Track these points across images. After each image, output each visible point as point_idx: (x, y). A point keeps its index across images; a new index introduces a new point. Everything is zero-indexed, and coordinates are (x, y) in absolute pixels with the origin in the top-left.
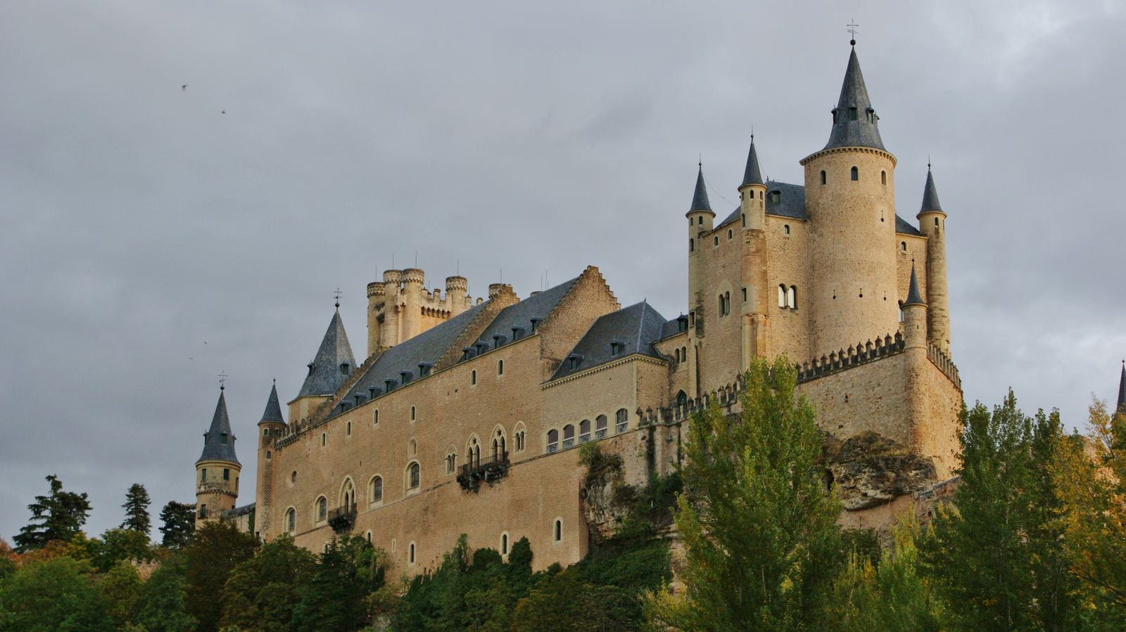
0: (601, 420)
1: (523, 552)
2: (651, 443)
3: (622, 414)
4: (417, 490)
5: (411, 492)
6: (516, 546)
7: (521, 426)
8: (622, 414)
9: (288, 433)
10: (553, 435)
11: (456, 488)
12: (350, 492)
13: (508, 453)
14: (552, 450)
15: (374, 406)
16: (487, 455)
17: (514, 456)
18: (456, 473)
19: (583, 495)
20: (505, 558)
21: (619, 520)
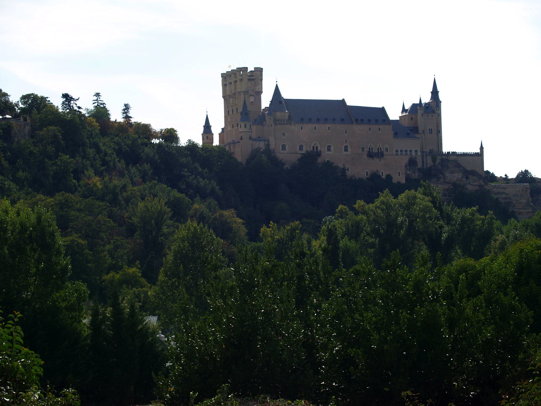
0: (411, 151)
1: (389, 177)
2: (423, 159)
3: (416, 151)
4: (348, 153)
5: (345, 153)
6: (387, 175)
7: (386, 146)
8: (416, 151)
9: (284, 121)
10: (397, 151)
11: (365, 156)
12: (315, 147)
13: (383, 152)
14: (397, 154)
15: (327, 126)
16: (375, 151)
17: (385, 153)
18: (366, 152)
19: (406, 166)
20: (384, 177)
21: (419, 176)
